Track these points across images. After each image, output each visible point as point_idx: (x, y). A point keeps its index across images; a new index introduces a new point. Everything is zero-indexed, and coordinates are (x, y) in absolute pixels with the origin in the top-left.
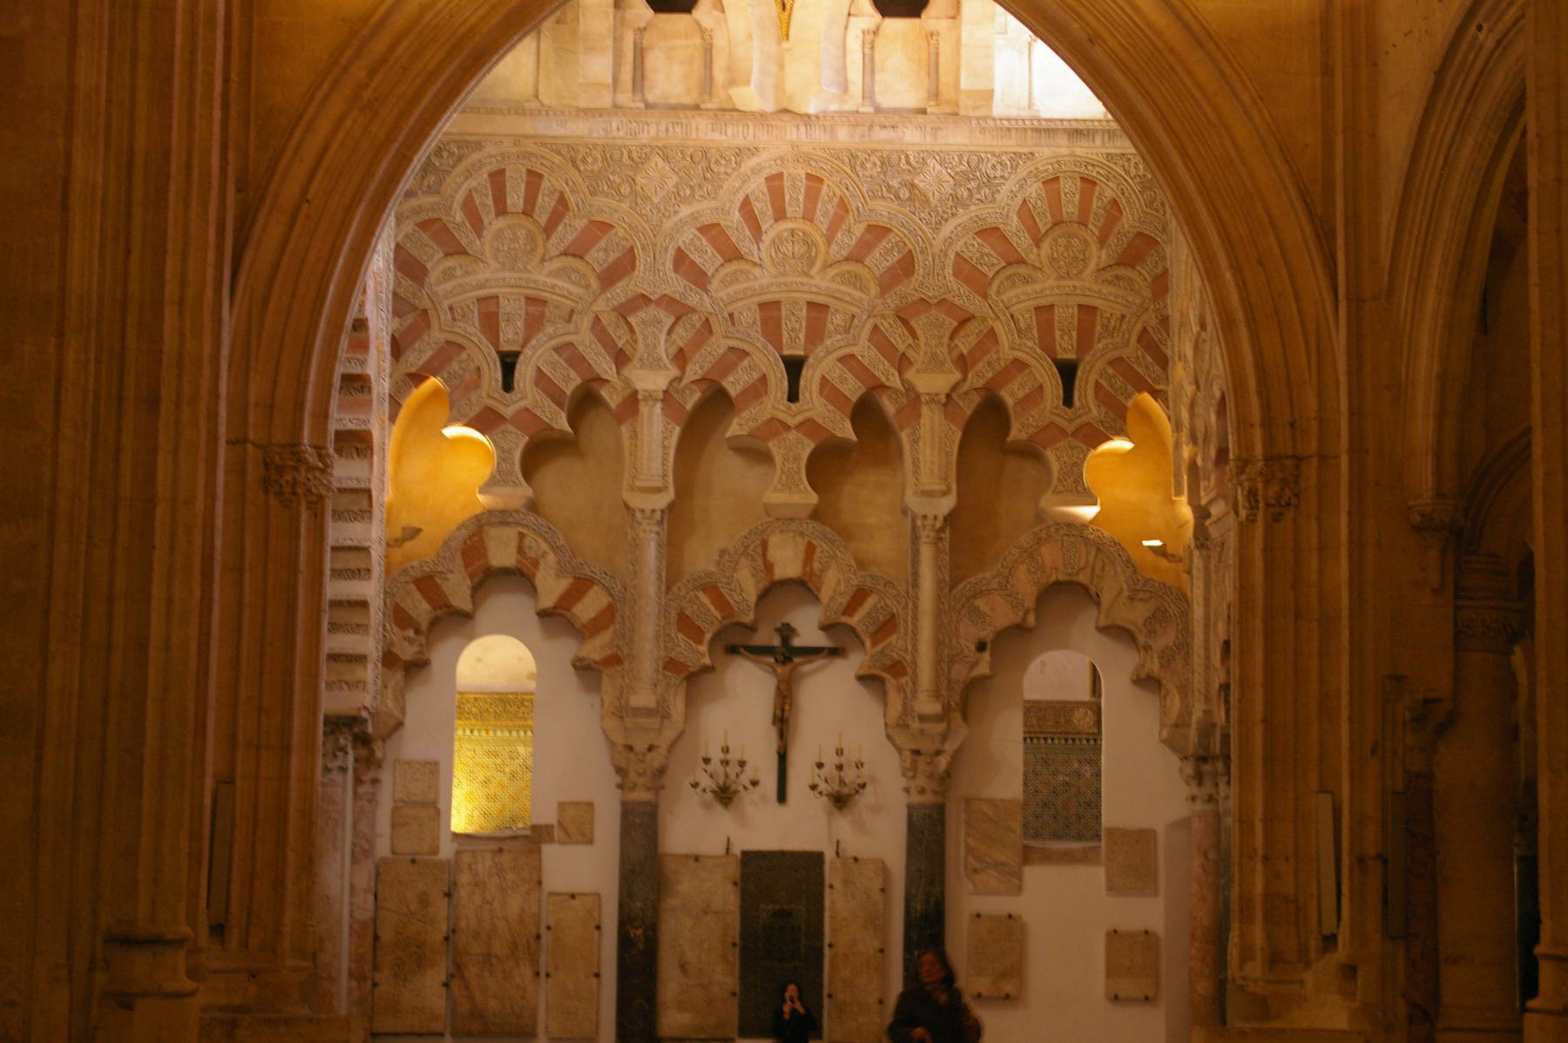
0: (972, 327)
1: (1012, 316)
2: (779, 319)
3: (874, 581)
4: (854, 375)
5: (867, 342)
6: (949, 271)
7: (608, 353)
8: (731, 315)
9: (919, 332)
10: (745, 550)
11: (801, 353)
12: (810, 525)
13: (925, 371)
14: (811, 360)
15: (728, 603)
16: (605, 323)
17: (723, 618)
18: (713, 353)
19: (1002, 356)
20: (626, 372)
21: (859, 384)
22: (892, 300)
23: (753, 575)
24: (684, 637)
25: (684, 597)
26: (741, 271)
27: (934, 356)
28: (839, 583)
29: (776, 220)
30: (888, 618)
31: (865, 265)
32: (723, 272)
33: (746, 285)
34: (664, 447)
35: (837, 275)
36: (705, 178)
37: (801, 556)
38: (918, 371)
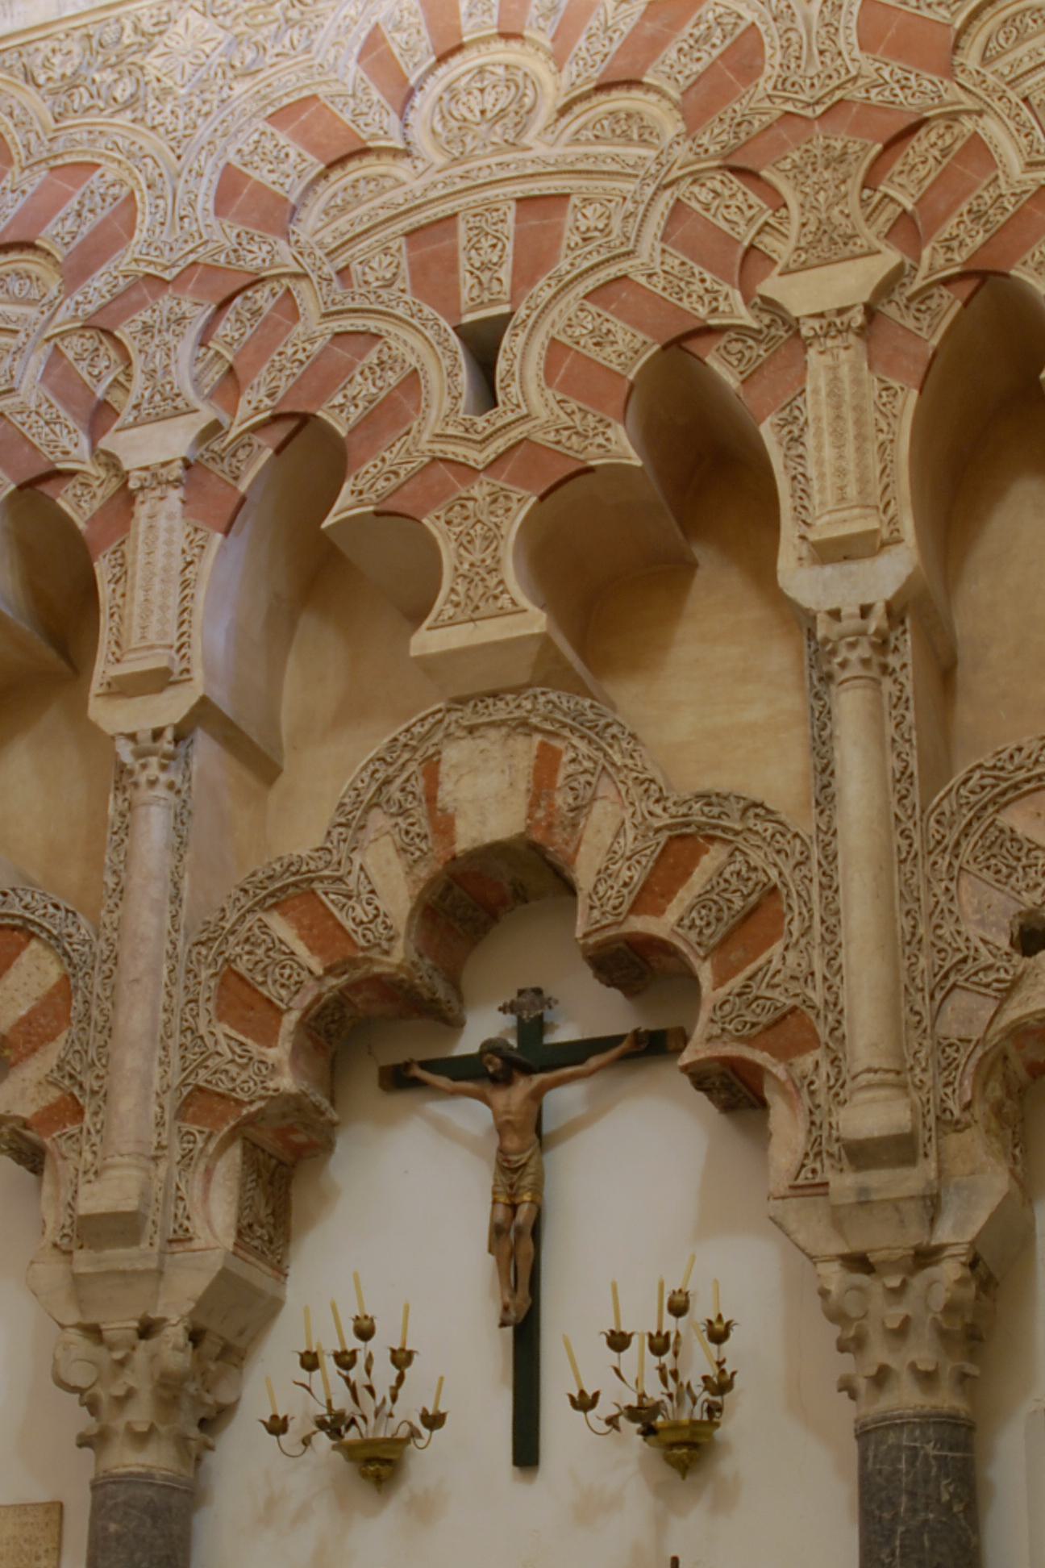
0: (921, 145)
1: (1026, 100)
2: (455, 250)
3: (716, 810)
4: (628, 322)
5: (659, 246)
6: (848, 38)
7: (75, 415)
8: (343, 273)
9: (785, 188)
10: (379, 790)
11: (505, 309)
12: (542, 699)
13: (805, 267)
14: (522, 312)
15: (340, 926)
16: (70, 355)
17: (329, 971)
18: (301, 356)
19: (1004, 190)
20: (104, 443)
21: (641, 337)
22: (715, 138)
23: (402, 851)
24: (233, 1033)
25: (233, 932)
26: (367, 180)
27: (824, 230)
28: (620, 832)
29: (442, 59)
30: (754, 898)
31: (649, 88)
32: (326, 192)
33: (378, 202)
34: (185, 584)
35: (584, 127)
36: (287, 20)
37: (523, 786)
38: (786, 272)
